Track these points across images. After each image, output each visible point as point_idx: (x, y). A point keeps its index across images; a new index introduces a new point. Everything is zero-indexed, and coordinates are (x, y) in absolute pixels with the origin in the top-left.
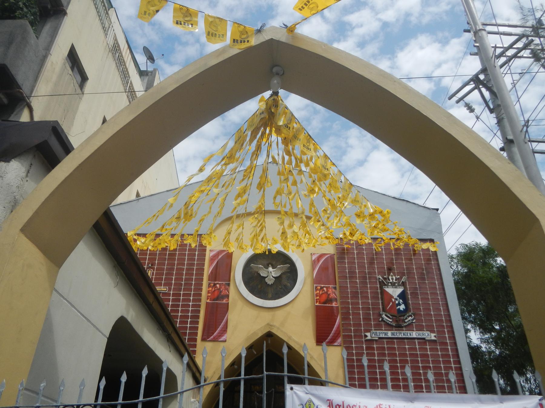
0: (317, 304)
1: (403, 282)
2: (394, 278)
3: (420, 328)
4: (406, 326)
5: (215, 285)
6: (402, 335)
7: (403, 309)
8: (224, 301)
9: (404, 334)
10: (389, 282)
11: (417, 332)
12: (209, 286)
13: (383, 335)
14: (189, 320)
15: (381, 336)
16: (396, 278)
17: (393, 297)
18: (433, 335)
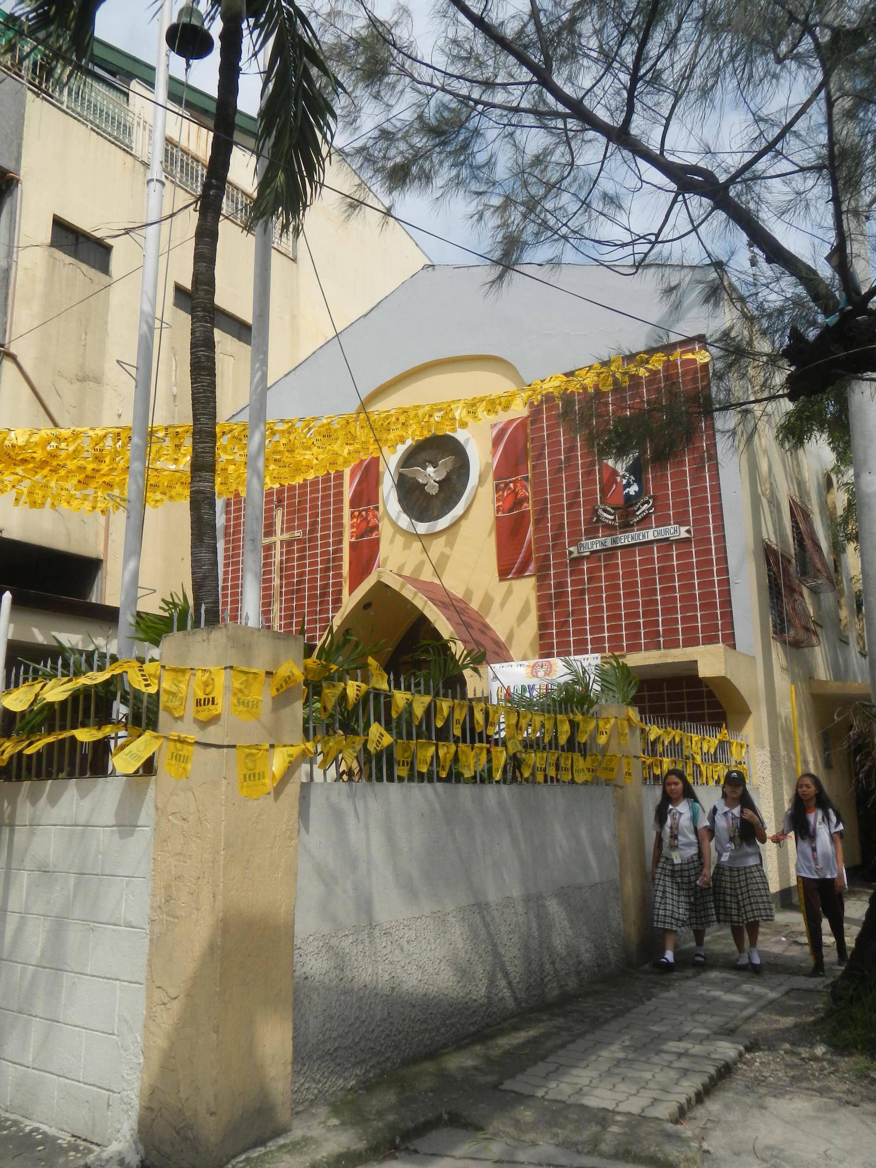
3: (663, 521)
4: (638, 522)
6: (630, 539)
9: (632, 538)
12: (352, 516)
15: (595, 548)
18: (684, 529)
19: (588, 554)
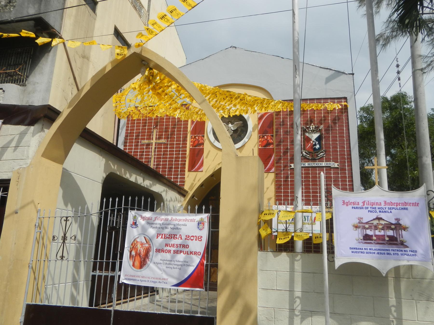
0: (260, 147)
1: (320, 129)
2: (314, 126)
3: (328, 160)
4: (318, 159)
5: (195, 137)
6: (315, 165)
7: (318, 148)
8: (201, 147)
9: (316, 164)
10: (310, 130)
12: (192, 138)
14: (180, 159)
16: (315, 127)
18: (336, 164)
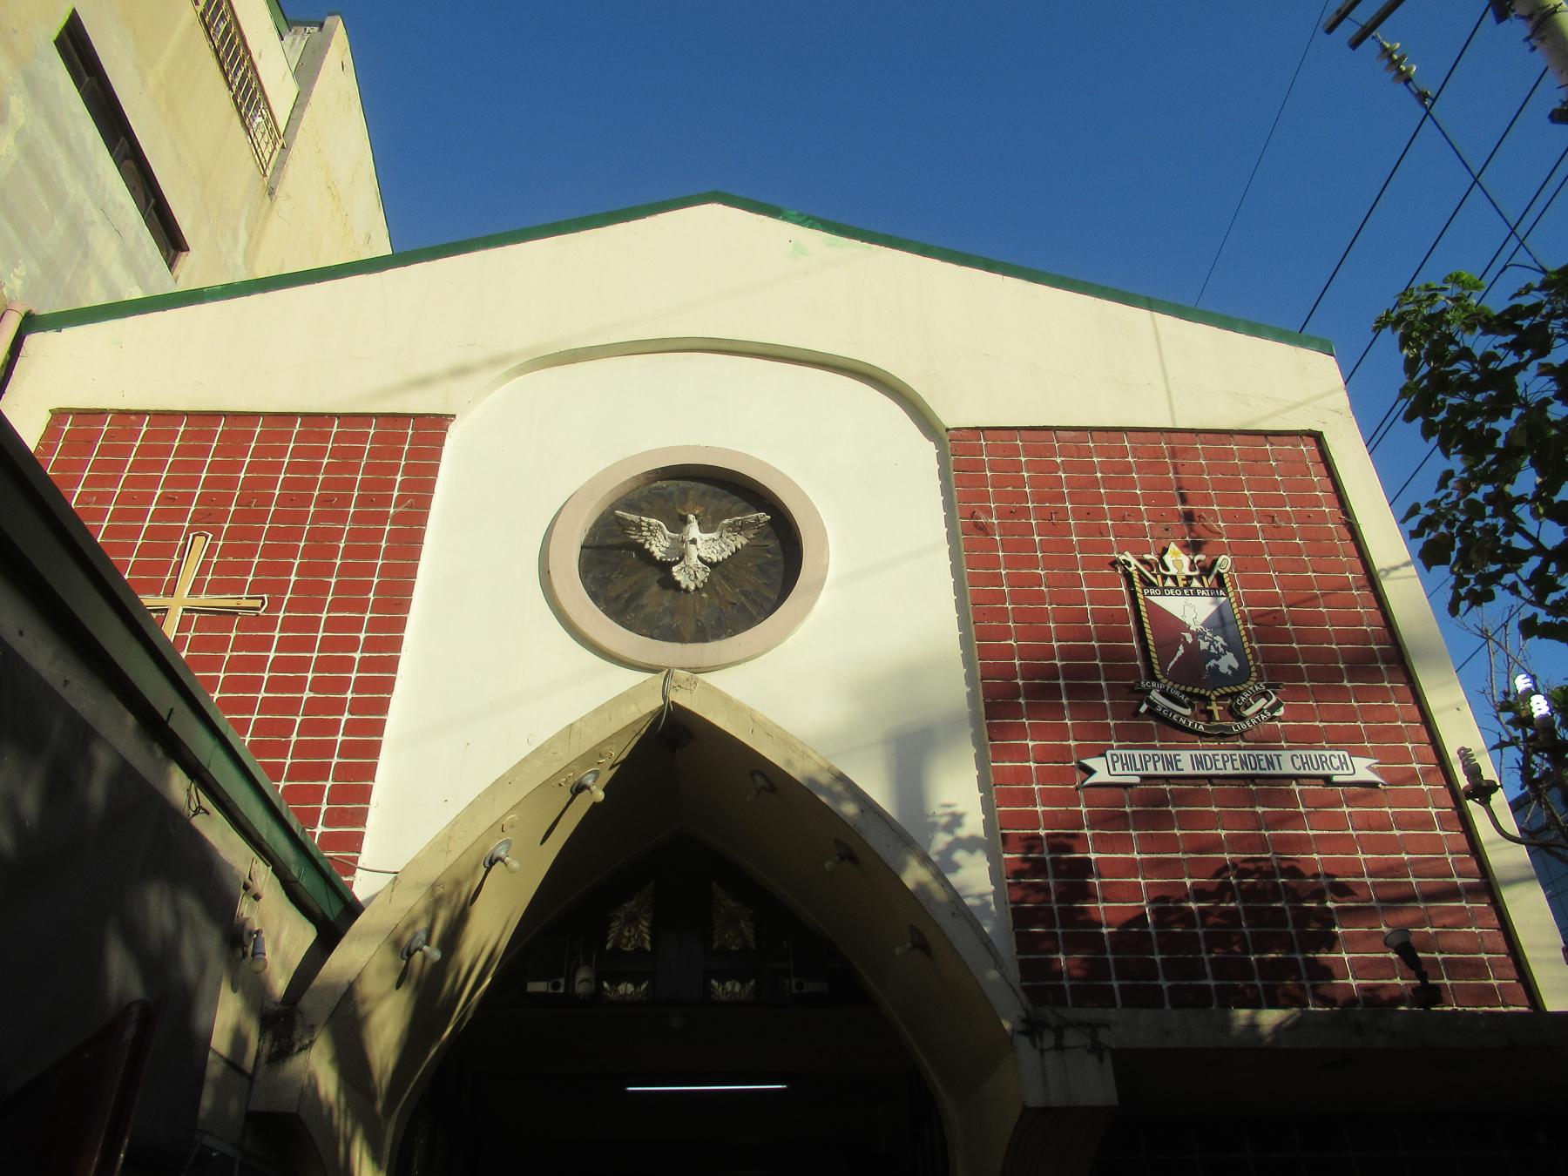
6: (1237, 764)
7: (1230, 667)
9: (1243, 763)
11: (1298, 753)
13: (1159, 765)
15: (1151, 771)
17: (1188, 630)
19: (1137, 780)
